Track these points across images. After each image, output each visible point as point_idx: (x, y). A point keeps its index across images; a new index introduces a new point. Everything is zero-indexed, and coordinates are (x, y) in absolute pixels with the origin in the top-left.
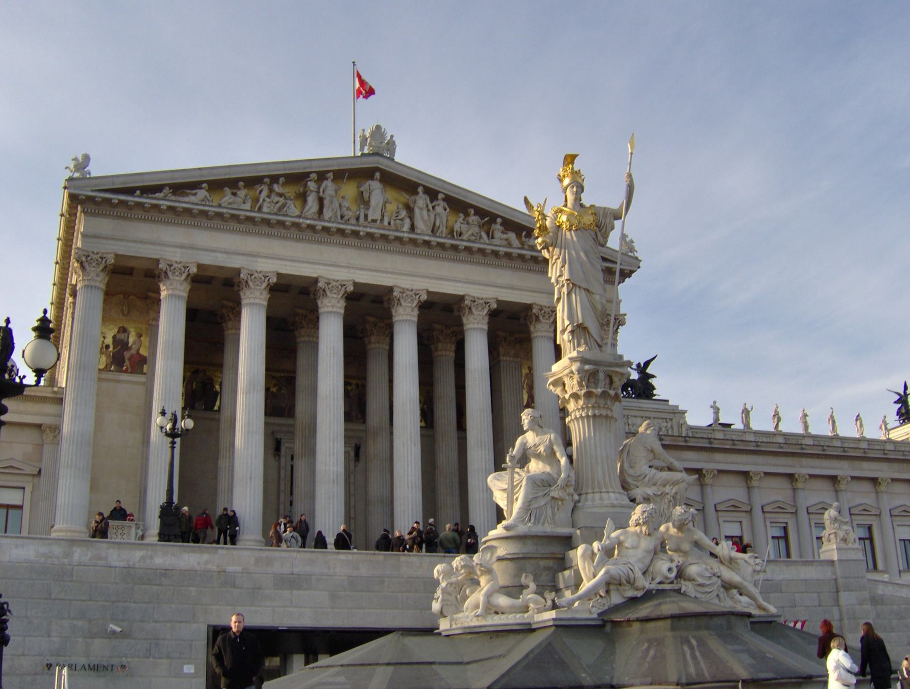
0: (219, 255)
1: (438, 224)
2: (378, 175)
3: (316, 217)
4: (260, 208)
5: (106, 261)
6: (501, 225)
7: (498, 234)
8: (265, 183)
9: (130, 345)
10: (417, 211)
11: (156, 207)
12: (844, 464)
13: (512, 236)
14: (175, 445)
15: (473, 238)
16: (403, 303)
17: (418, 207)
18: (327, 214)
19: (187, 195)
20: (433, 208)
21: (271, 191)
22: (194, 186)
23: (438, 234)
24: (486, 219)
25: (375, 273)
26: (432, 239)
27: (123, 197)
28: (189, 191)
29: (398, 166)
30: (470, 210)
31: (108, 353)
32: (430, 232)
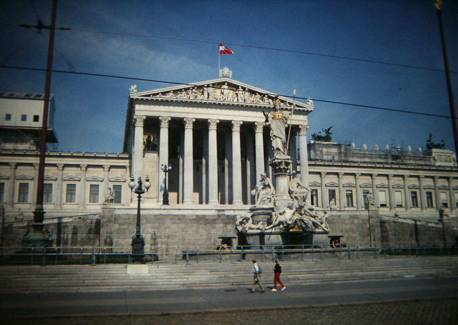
0: (177, 113)
1: (246, 99)
2: (226, 84)
3: (207, 99)
6: (267, 97)
7: (266, 101)
10: (239, 95)
11: (157, 100)
12: (392, 170)
13: (270, 101)
15: (257, 103)
18: (210, 97)
19: (167, 95)
20: (244, 93)
22: (169, 92)
23: (246, 102)
26: (244, 104)
28: (167, 94)
32: (243, 102)
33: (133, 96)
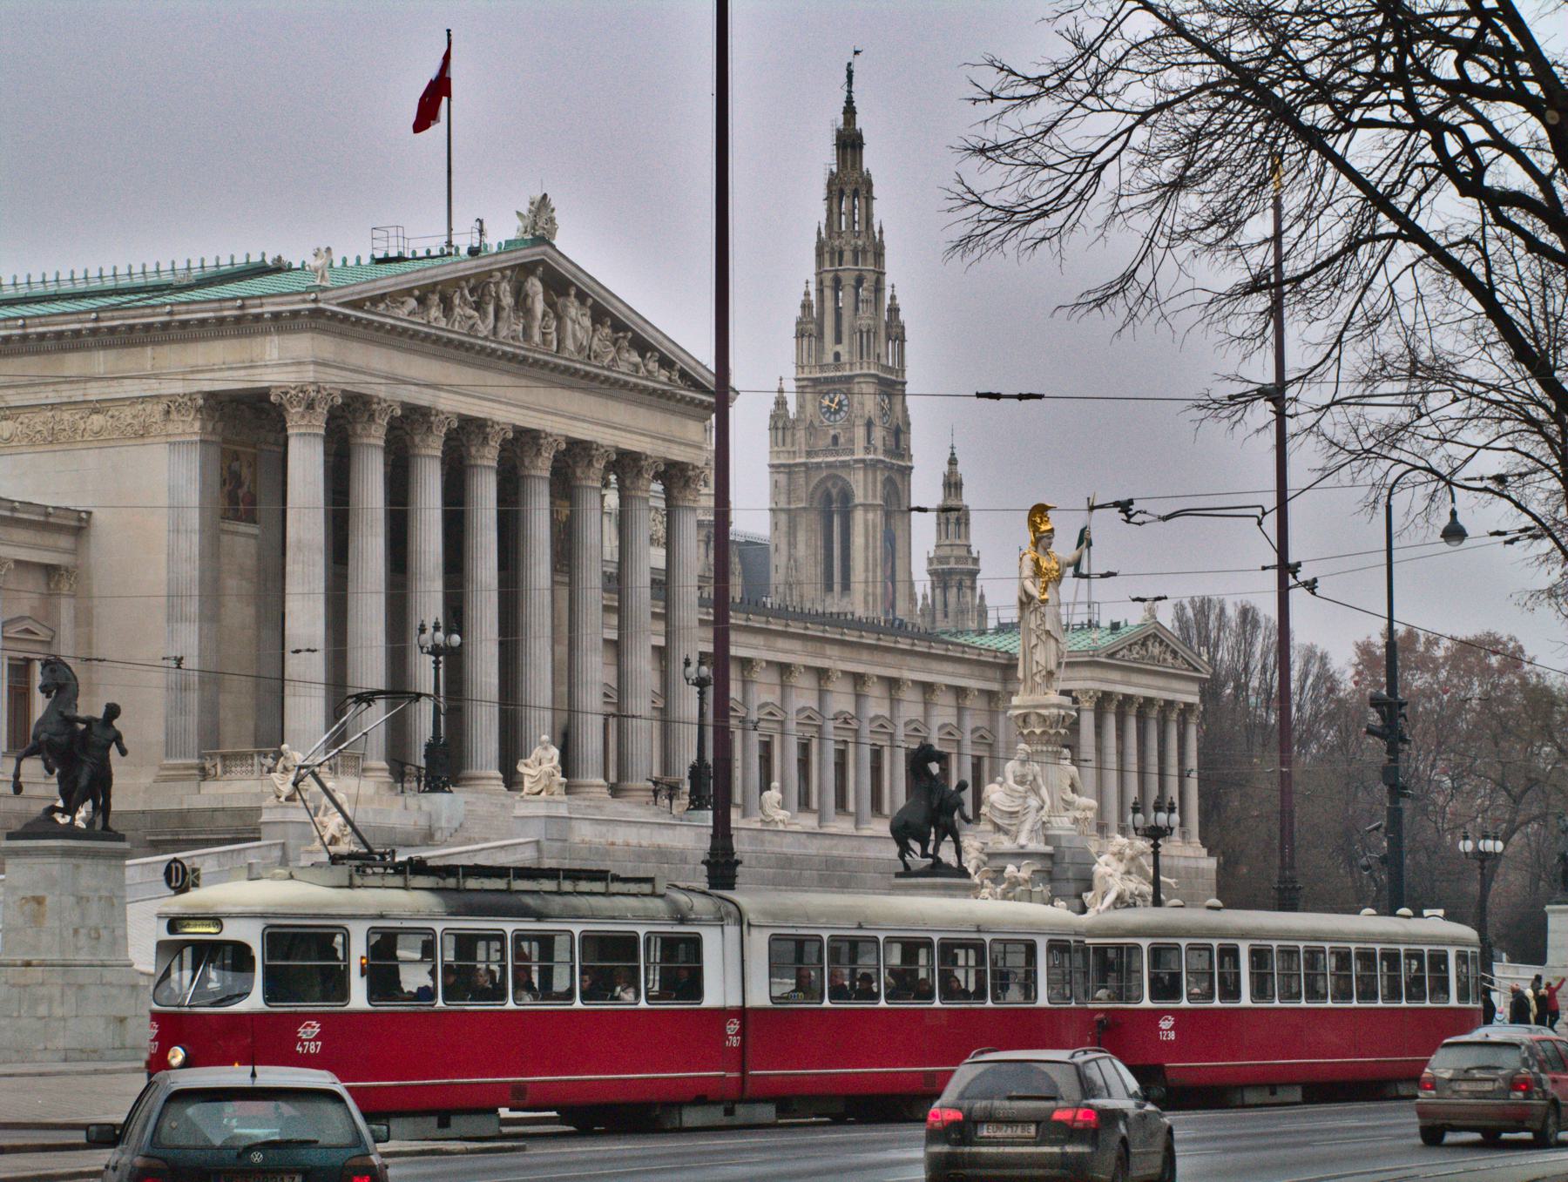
0: (413, 388)
4: (453, 325)
10: (569, 323)
13: (636, 358)
17: (571, 319)
18: (503, 332)
21: (462, 296)
22: (408, 292)
24: (621, 334)
25: (525, 412)
26: (582, 367)
27: (359, 314)
29: (561, 260)
33: (326, 301)
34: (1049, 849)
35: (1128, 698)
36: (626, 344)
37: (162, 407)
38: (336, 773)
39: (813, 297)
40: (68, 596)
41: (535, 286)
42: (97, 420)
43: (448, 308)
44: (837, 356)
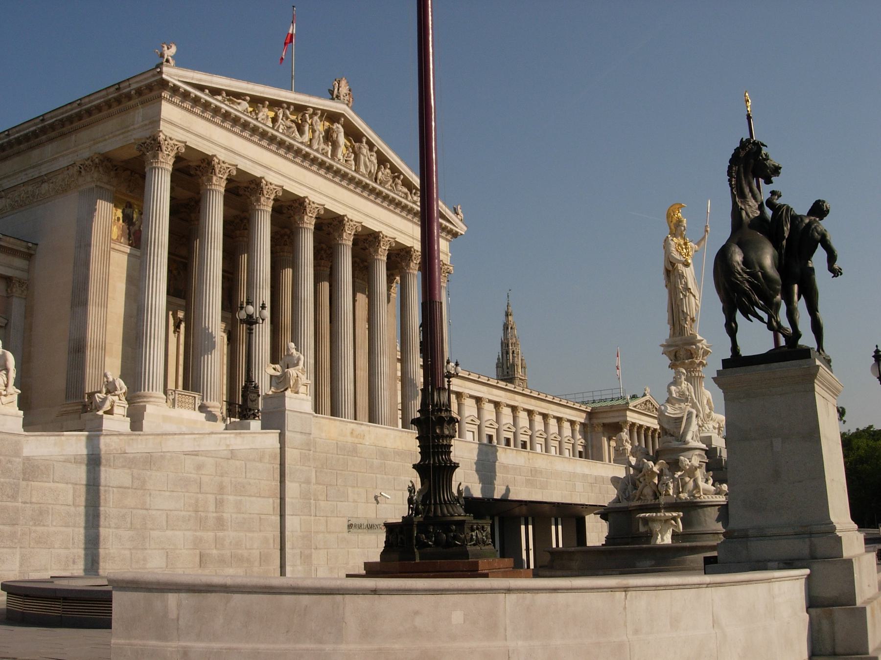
0: (248, 162)
1: (373, 171)
5: (178, 149)
6: (401, 181)
8: (283, 108)
9: (134, 220)
10: (362, 157)
13: (405, 190)
14: (252, 331)
16: (347, 231)
19: (233, 102)
21: (285, 114)
24: (396, 174)
27: (199, 93)
28: (235, 100)
30: (387, 163)
31: (119, 225)
34: (704, 446)
35: (641, 426)
36: (400, 182)
37: (76, 168)
38: (174, 406)
39: (500, 356)
40: (16, 297)
41: (339, 130)
42: (45, 187)
43: (274, 120)
44: (508, 373)
